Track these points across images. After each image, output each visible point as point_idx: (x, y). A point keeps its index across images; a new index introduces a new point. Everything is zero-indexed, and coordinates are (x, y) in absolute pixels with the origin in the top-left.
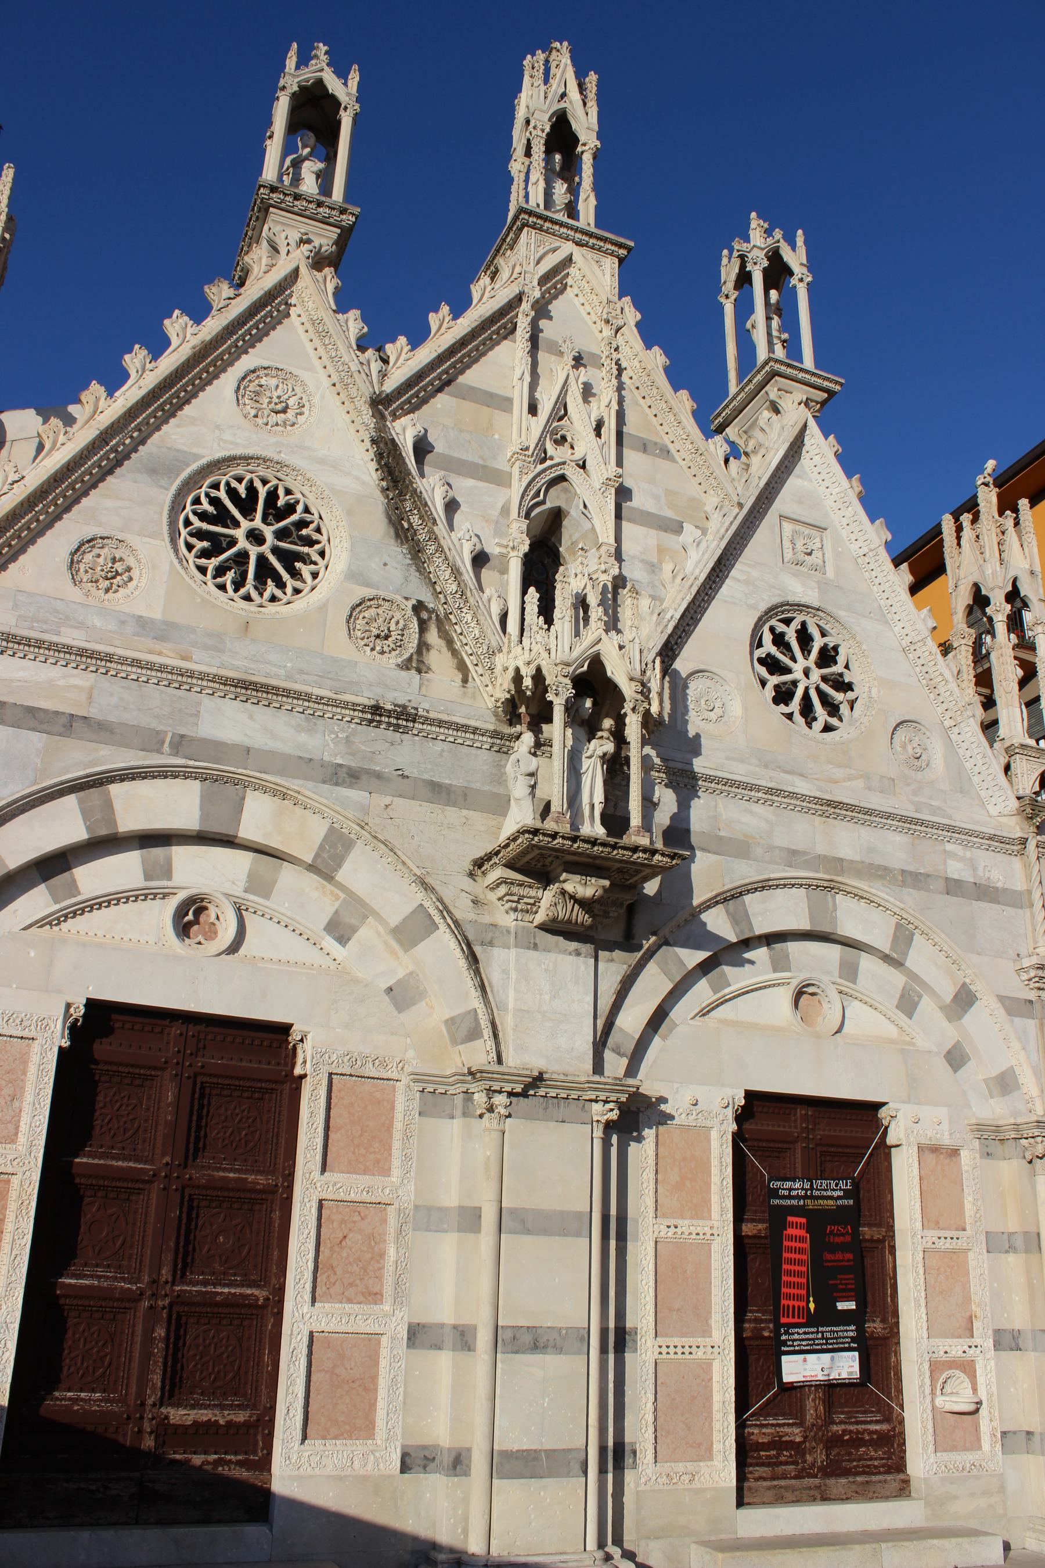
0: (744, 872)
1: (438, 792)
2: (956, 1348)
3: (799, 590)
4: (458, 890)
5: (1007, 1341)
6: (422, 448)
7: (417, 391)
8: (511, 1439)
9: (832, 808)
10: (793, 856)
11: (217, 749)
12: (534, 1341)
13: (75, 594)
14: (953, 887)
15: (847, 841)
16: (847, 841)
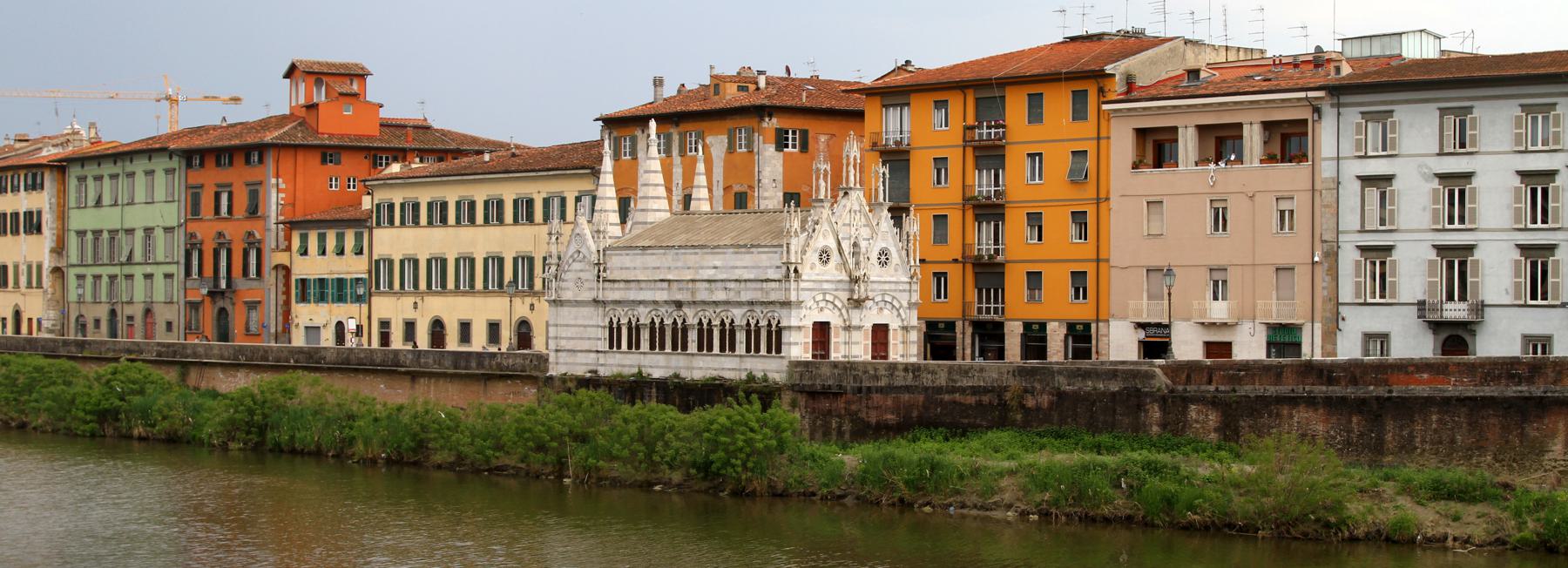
15: (887, 287)
16: (887, 287)
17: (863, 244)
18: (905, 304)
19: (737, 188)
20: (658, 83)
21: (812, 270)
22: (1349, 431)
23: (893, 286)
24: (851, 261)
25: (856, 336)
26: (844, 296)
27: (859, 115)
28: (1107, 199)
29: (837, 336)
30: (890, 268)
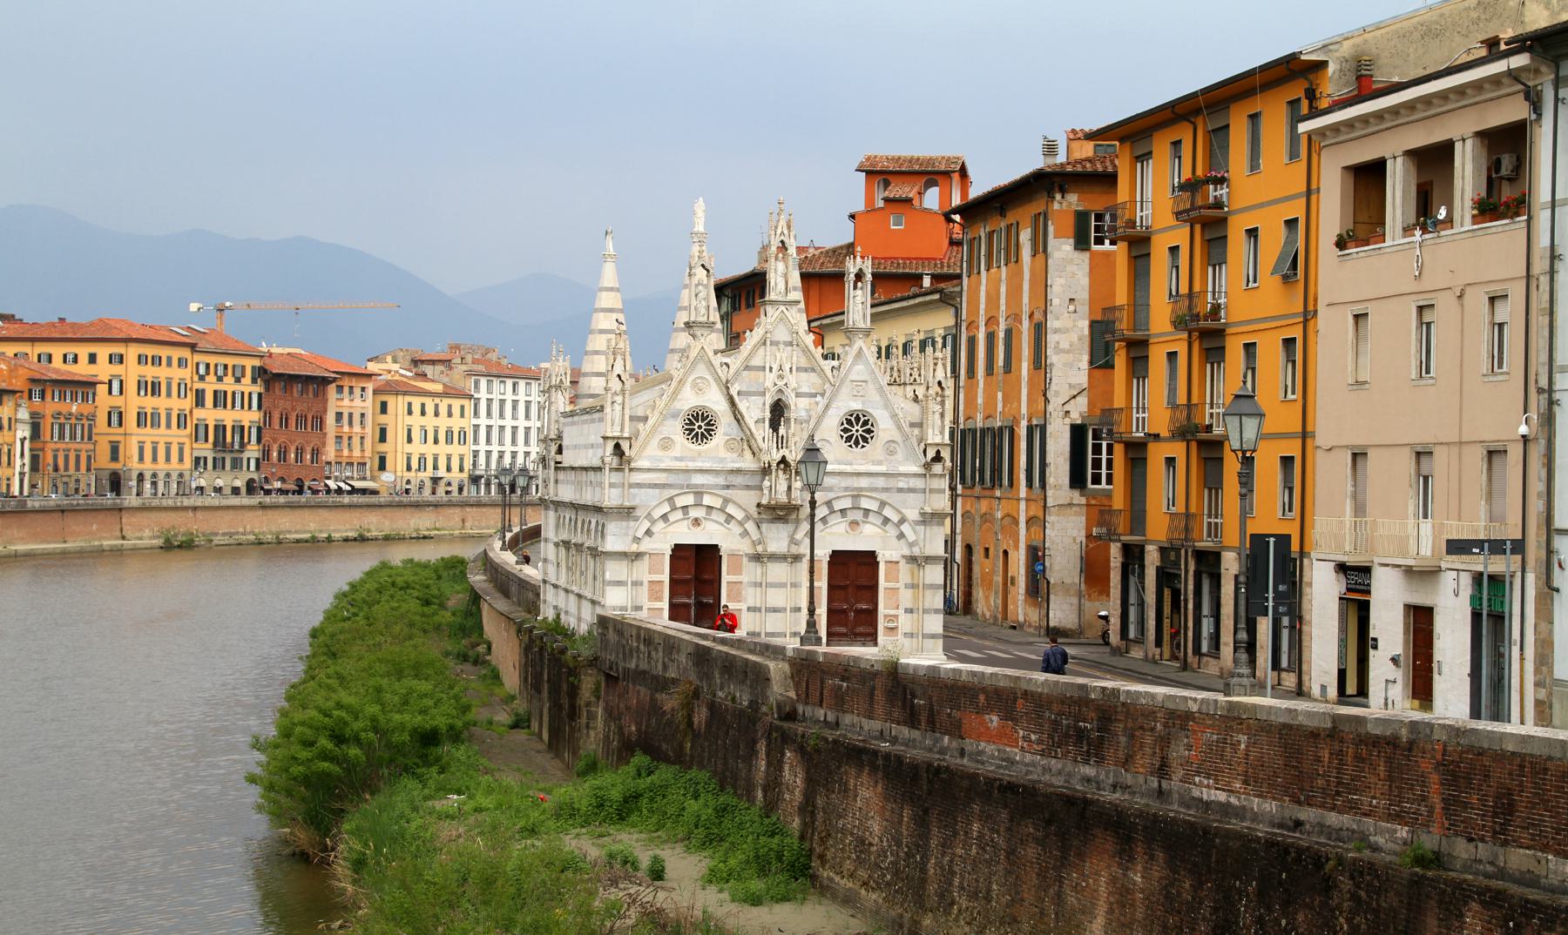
0: (831, 495)
1: (748, 487)
2: (892, 612)
3: (856, 405)
4: (753, 511)
5: (906, 611)
6: (739, 393)
7: (737, 373)
8: (769, 630)
9: (859, 474)
10: (846, 489)
11: (696, 486)
12: (775, 610)
13: (660, 453)
14: (900, 490)
15: (864, 483)
16: (864, 483)
17: (798, 407)
18: (913, 514)
19: (1038, 316)
20: (1050, 149)
21: (663, 449)
22: (899, 844)
23: (880, 482)
24: (762, 433)
25: (778, 571)
26: (749, 499)
27: (1108, 180)
28: (1316, 312)
29: (737, 569)
30: (875, 447)
